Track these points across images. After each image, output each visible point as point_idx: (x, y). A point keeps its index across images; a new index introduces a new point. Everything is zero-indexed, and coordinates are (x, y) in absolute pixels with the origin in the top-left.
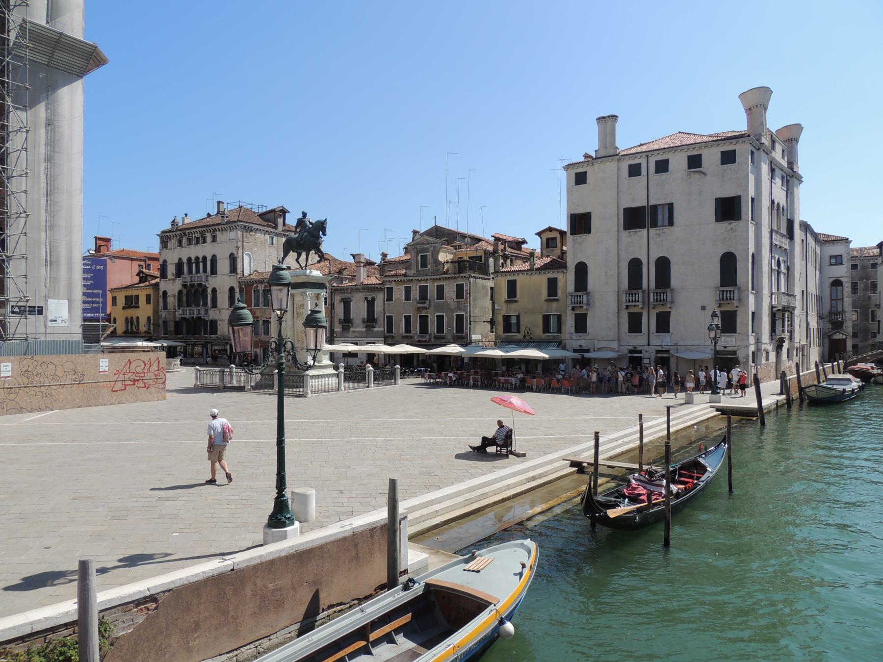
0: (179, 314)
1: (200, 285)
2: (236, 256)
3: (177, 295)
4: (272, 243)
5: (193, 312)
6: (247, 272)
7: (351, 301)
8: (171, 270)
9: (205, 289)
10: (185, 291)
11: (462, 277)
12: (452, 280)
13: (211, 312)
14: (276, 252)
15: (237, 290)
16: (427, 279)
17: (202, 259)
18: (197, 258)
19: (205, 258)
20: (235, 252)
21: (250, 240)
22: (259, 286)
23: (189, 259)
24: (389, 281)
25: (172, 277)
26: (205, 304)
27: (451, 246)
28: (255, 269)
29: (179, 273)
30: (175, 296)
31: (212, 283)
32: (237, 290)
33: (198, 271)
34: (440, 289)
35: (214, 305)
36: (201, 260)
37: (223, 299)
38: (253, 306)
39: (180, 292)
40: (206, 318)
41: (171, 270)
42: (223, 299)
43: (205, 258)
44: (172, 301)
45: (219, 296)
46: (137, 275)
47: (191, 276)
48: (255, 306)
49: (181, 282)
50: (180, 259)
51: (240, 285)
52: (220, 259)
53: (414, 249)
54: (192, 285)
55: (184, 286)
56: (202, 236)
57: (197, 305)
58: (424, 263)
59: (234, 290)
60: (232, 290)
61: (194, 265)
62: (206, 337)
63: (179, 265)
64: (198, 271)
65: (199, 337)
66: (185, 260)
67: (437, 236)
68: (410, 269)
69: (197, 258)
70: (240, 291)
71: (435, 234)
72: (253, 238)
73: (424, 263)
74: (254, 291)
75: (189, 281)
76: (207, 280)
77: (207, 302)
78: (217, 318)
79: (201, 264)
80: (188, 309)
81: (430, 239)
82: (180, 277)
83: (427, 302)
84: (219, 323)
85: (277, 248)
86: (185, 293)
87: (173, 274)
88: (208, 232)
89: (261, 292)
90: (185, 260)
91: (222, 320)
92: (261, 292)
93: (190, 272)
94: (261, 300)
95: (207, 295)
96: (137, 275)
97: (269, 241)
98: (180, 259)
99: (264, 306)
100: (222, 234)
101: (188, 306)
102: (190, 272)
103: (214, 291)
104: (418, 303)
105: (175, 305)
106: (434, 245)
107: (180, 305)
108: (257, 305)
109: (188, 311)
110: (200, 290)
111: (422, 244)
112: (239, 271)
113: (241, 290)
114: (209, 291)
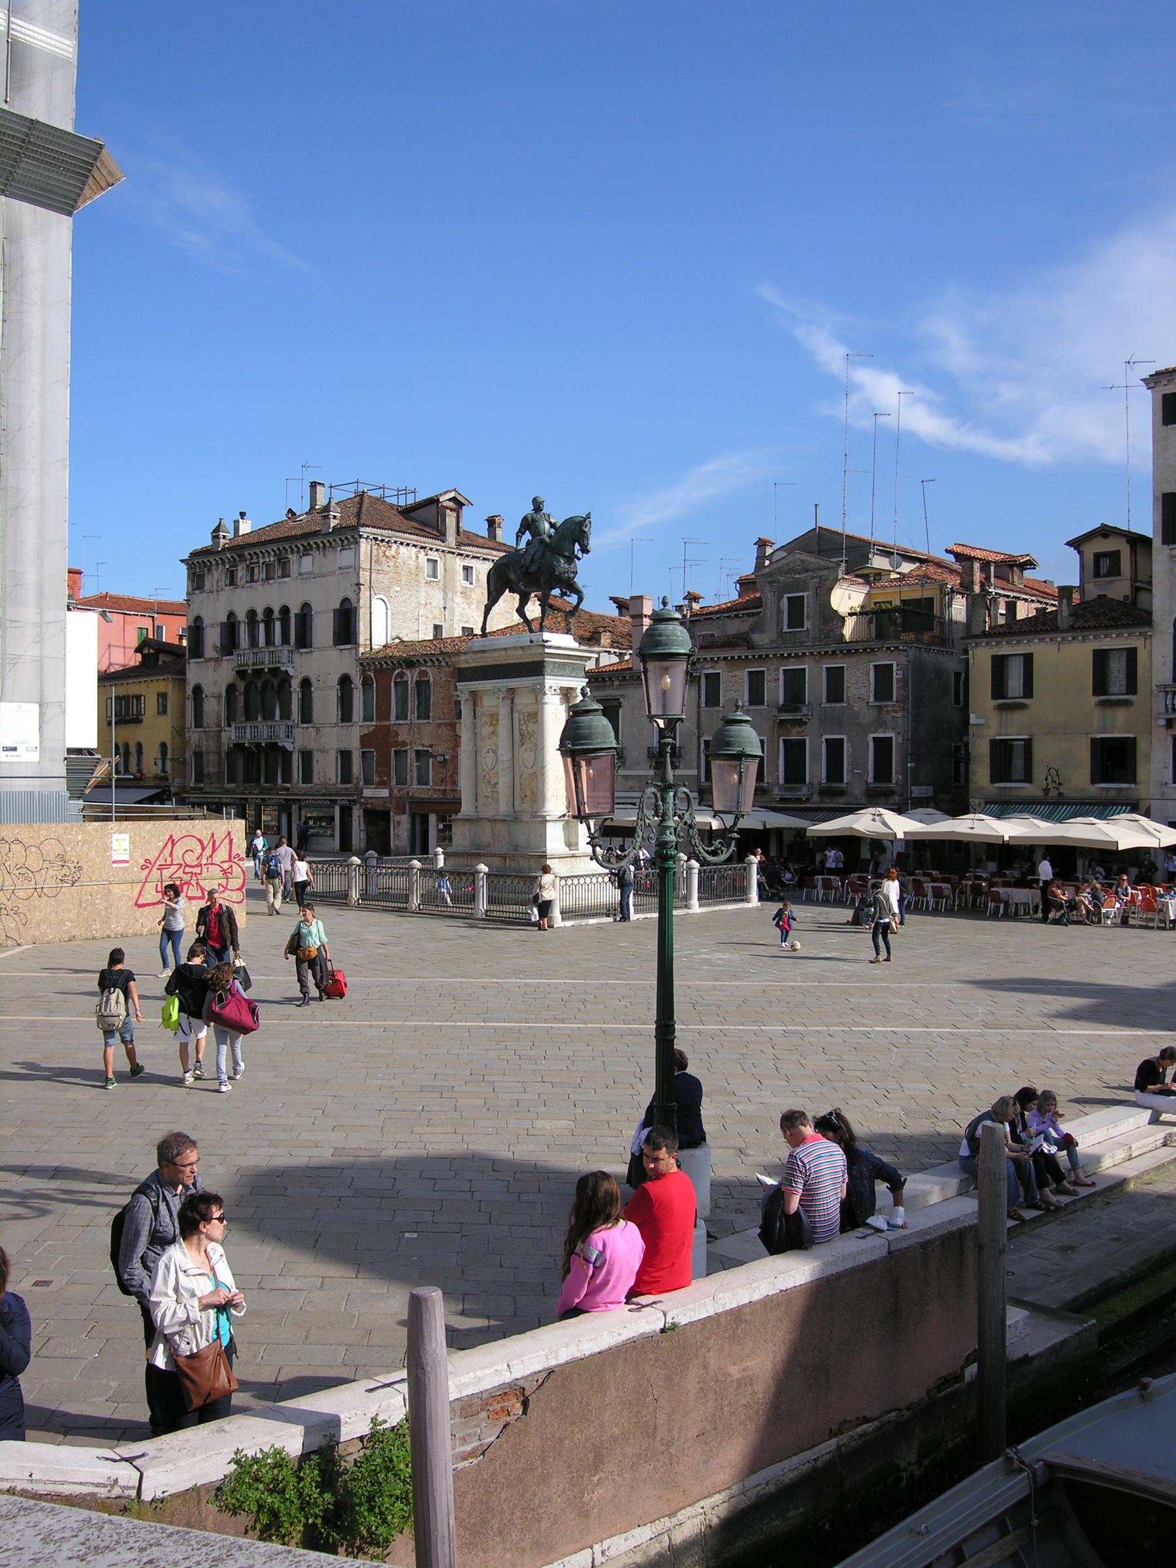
0: (230, 735)
1: (275, 671)
2: (355, 604)
3: (224, 694)
4: (435, 576)
5: (258, 732)
6: (379, 641)
7: (620, 706)
8: (212, 638)
9: (286, 679)
10: (241, 686)
11: (888, 648)
12: (865, 657)
13: (297, 732)
14: (440, 595)
15: (357, 681)
16: (767, 656)
17: (280, 613)
18: (269, 611)
19: (285, 610)
20: (351, 595)
21: (385, 568)
22: (408, 672)
23: (252, 614)
24: (712, 659)
25: (214, 655)
26: (286, 715)
27: (857, 576)
28: (395, 635)
29: (229, 644)
30: (220, 696)
31: (298, 667)
32: (357, 681)
33: (269, 641)
34: (835, 679)
35: (307, 717)
36: (276, 614)
37: (326, 702)
38: (393, 717)
39: (231, 688)
40: (289, 747)
41: (212, 638)
42: (326, 702)
43: (285, 610)
44: (213, 708)
45: (316, 695)
46: (136, 651)
47: (256, 650)
48: (397, 718)
49: (235, 664)
50: (231, 614)
51: (363, 672)
52: (319, 613)
53: (771, 583)
54: (258, 673)
55: (241, 674)
56: (279, 560)
57: (269, 716)
58: (796, 618)
59: (351, 683)
60: (345, 681)
61: (262, 626)
62: (288, 789)
63: (230, 628)
64: (269, 641)
65: (271, 789)
66: (241, 616)
67: (822, 552)
68: (762, 631)
69: (269, 611)
70: (363, 685)
71: (816, 549)
72: (391, 564)
73: (796, 618)
74: (396, 683)
75: (251, 663)
76: (291, 661)
77: (290, 709)
78: (311, 745)
79: (278, 625)
80: (249, 724)
81: (813, 560)
82: (232, 654)
83: (804, 710)
84: (316, 756)
85: (445, 587)
86: (242, 690)
87: (215, 646)
88: (292, 552)
89: (411, 686)
90: (241, 616)
91: (323, 751)
92: (411, 686)
93: (254, 643)
94: (412, 703)
95: (290, 693)
96: (136, 651)
97: (426, 568)
98: (231, 614)
99: (419, 718)
100: (324, 555)
101: (248, 719)
102: (254, 643)
103: (306, 683)
104: (780, 710)
105: (219, 717)
106: (822, 573)
107: (231, 718)
108: (402, 715)
109: (248, 731)
110: (276, 682)
111: (792, 571)
112: (362, 638)
113: (366, 683)
114: (295, 684)
